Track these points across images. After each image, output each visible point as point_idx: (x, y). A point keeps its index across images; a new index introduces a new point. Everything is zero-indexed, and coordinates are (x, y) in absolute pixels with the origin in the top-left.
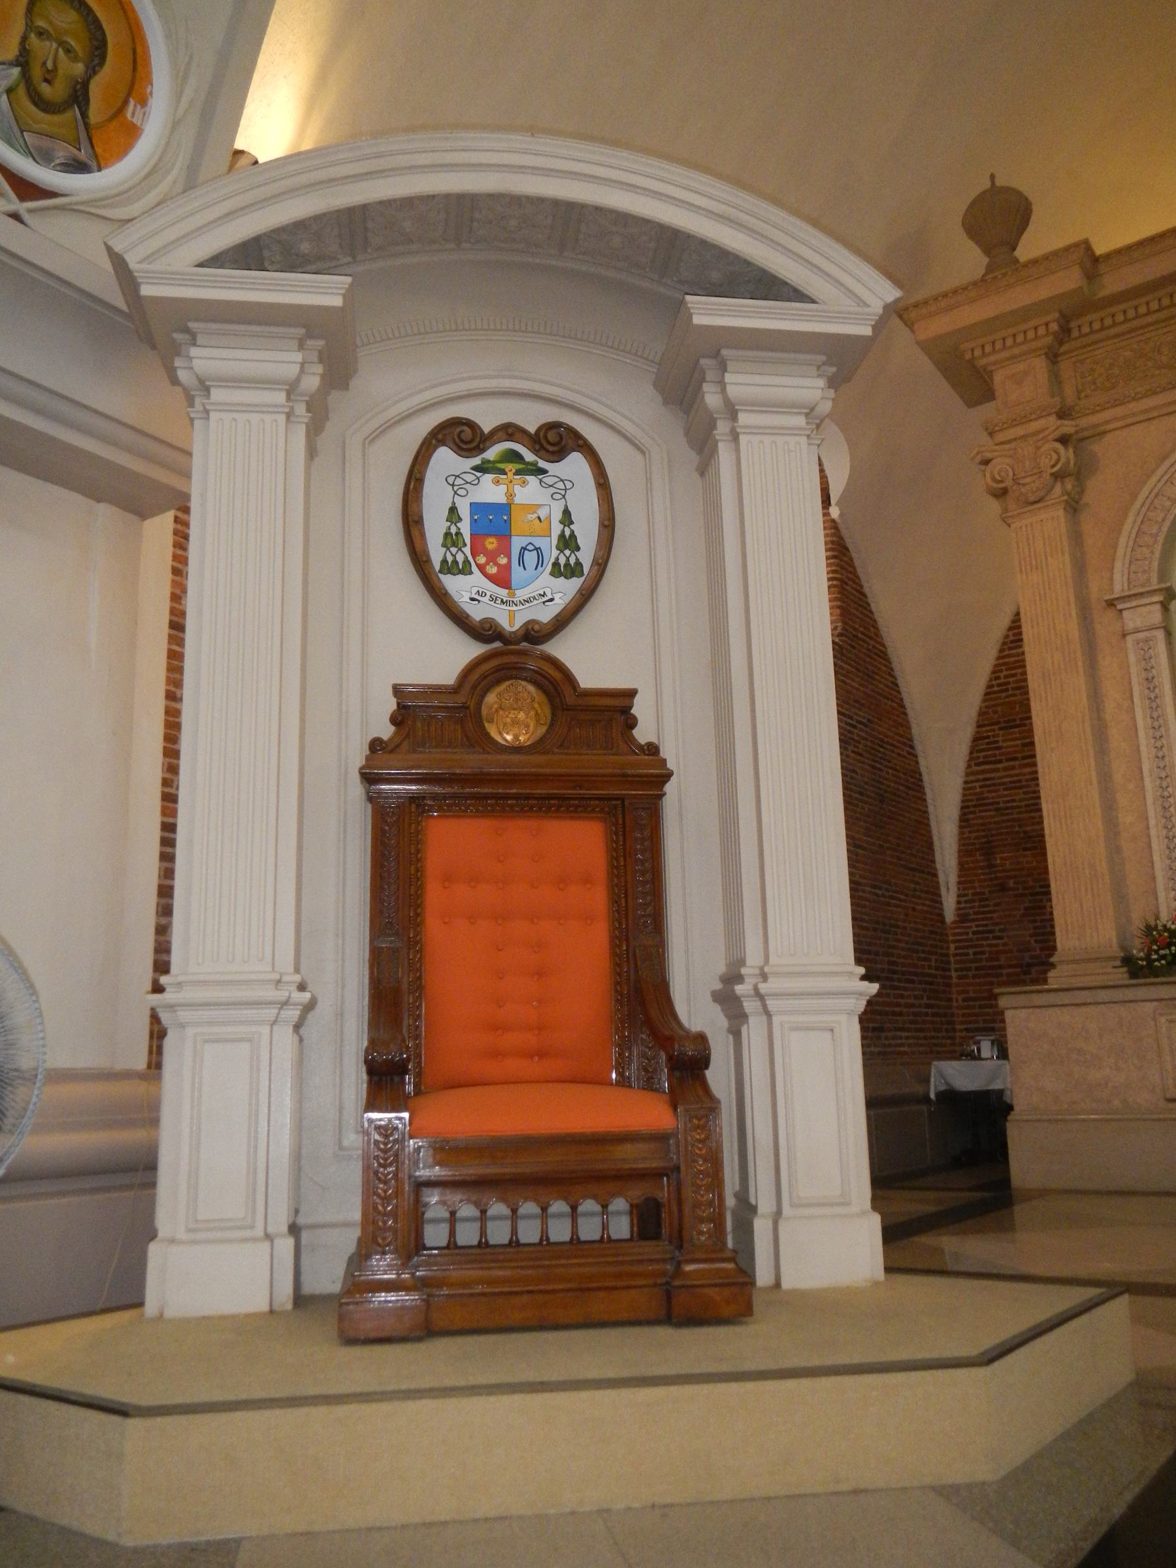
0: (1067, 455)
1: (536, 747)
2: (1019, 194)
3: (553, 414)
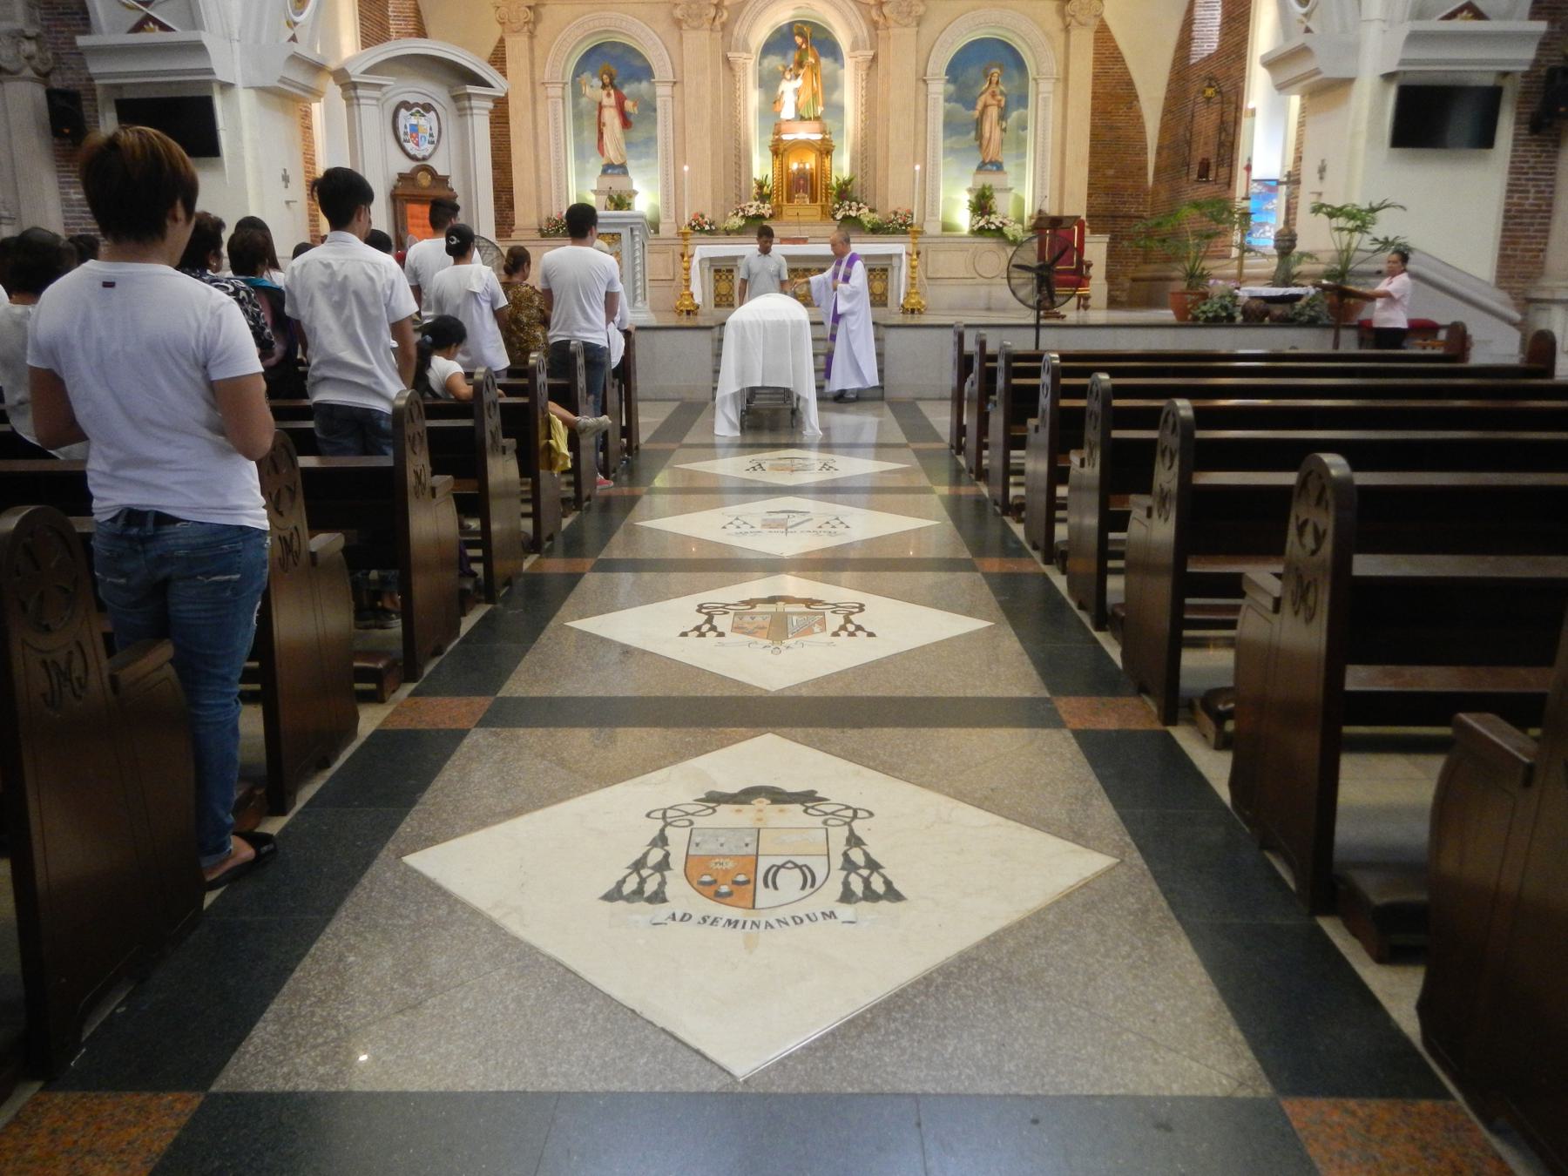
0: (531, 15)
1: (429, 188)
3: (429, 101)
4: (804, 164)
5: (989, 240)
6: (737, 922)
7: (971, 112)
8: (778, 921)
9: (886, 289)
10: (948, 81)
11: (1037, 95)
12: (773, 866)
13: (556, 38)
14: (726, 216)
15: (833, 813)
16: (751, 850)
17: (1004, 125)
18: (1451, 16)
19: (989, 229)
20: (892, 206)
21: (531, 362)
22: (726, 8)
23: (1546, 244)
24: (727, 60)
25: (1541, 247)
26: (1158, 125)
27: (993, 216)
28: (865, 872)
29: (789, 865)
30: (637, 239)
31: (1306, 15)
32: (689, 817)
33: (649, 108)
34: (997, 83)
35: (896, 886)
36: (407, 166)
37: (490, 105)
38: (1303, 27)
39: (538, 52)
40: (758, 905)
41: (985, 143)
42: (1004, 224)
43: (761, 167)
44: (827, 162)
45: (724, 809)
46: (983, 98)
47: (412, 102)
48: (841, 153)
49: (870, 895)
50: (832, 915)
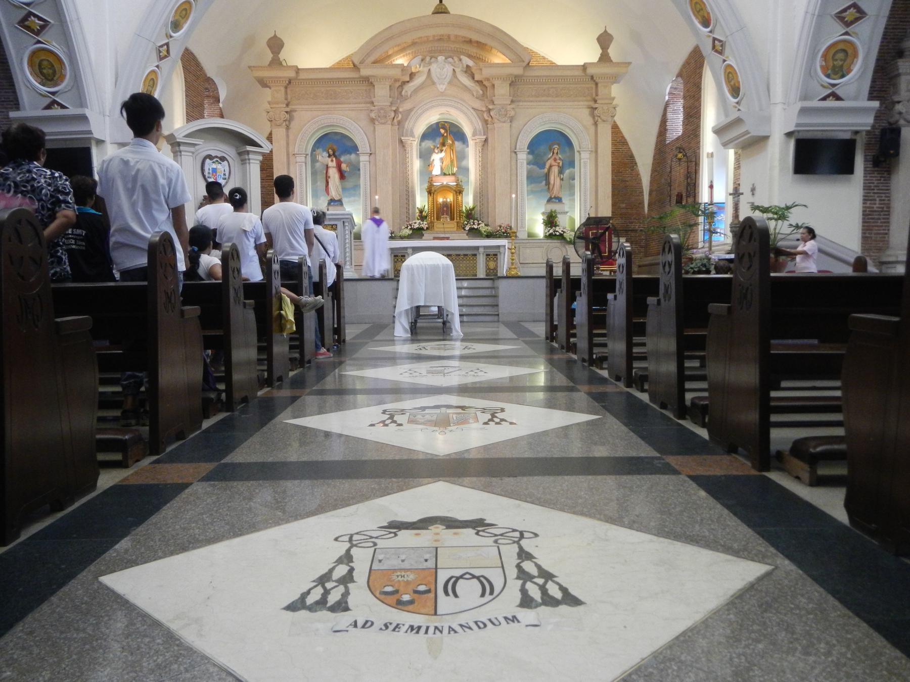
0: (287, 116)
2: (282, 41)
4: (446, 199)
5: (555, 241)
6: (419, 628)
7: (542, 170)
8: (461, 626)
9: (497, 266)
10: (529, 153)
11: (580, 160)
12: (452, 577)
13: (302, 129)
14: (401, 229)
15: (502, 535)
16: (431, 564)
17: (562, 176)
18: (824, 99)
19: (555, 235)
20: (498, 223)
21: (268, 256)
22: (401, 113)
23: (889, 230)
24: (401, 142)
25: (887, 232)
26: (649, 179)
27: (557, 227)
28: (541, 581)
29: (467, 576)
30: (347, 228)
31: (737, 103)
32: (373, 540)
33: (356, 168)
34: (557, 153)
35: (574, 591)
37: (261, 158)
38: (737, 109)
39: (291, 137)
40: (439, 612)
41: (551, 187)
42: (564, 232)
43: (421, 201)
44: (460, 198)
45: (404, 534)
46: (549, 161)
47: (213, 155)
48: (468, 194)
49: (549, 601)
50: (514, 619)
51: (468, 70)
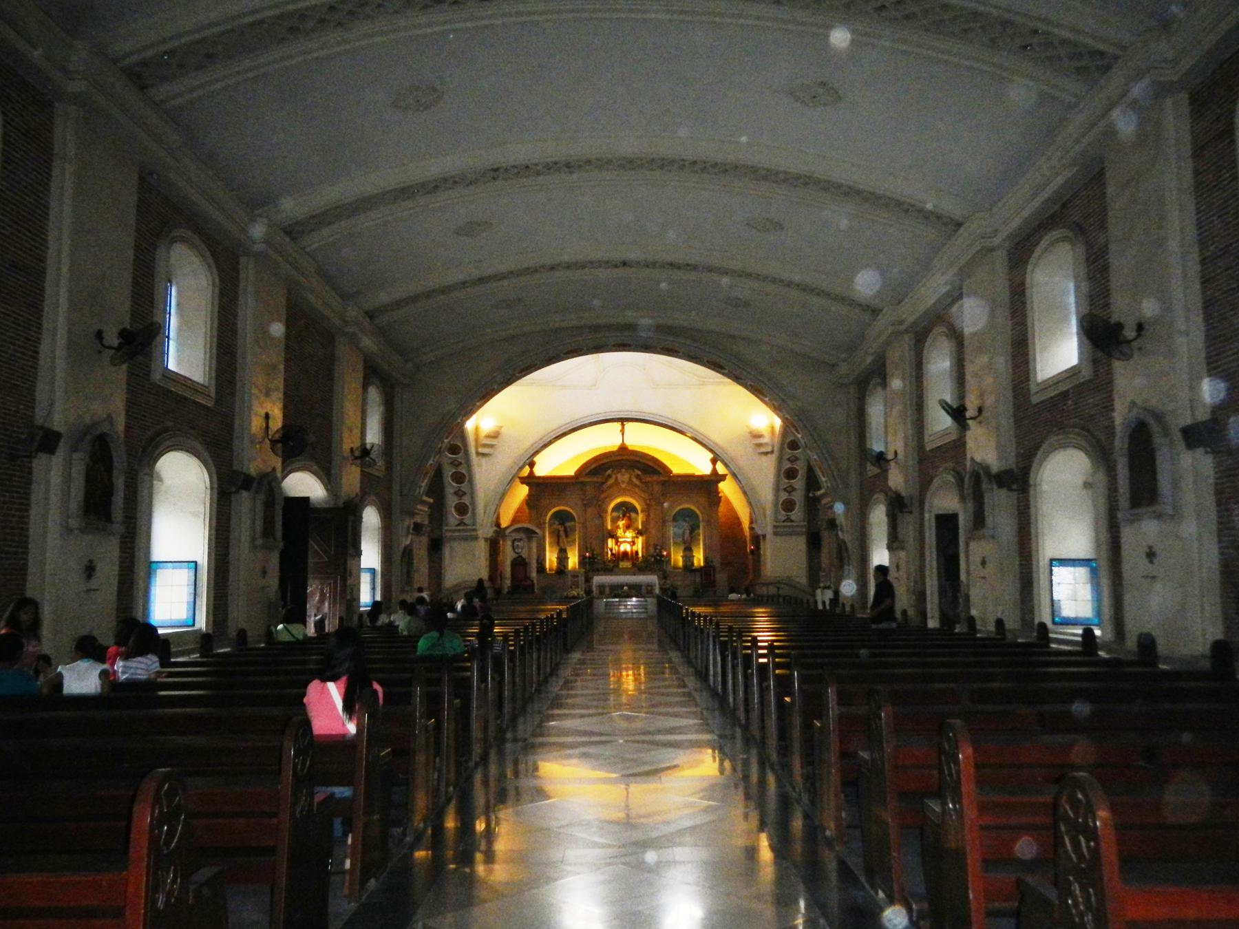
18: (784, 521)
36: (515, 556)
51: (638, 477)
